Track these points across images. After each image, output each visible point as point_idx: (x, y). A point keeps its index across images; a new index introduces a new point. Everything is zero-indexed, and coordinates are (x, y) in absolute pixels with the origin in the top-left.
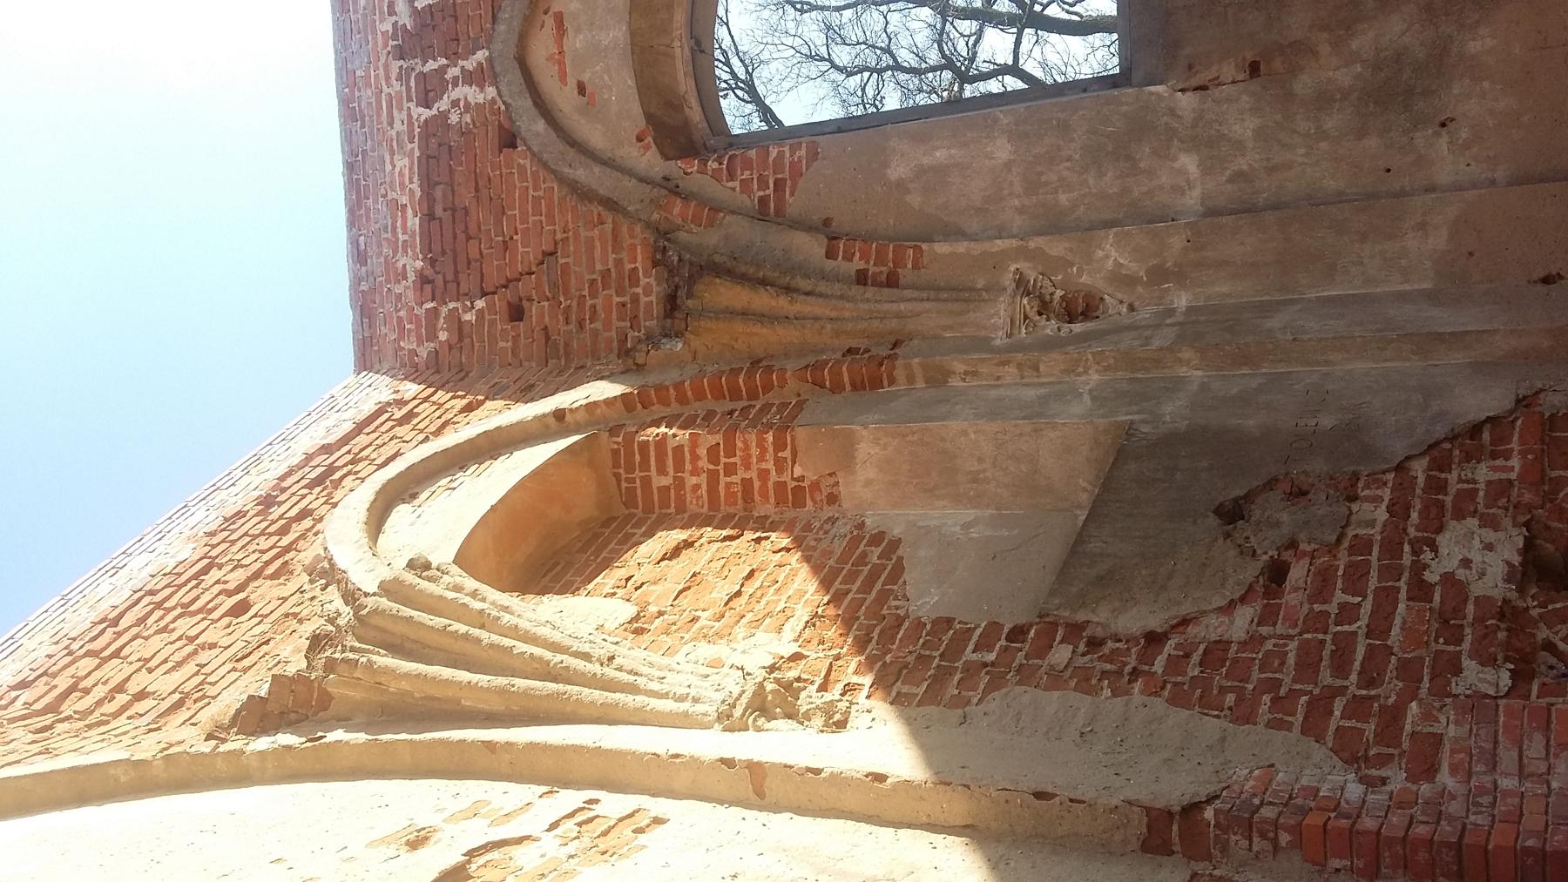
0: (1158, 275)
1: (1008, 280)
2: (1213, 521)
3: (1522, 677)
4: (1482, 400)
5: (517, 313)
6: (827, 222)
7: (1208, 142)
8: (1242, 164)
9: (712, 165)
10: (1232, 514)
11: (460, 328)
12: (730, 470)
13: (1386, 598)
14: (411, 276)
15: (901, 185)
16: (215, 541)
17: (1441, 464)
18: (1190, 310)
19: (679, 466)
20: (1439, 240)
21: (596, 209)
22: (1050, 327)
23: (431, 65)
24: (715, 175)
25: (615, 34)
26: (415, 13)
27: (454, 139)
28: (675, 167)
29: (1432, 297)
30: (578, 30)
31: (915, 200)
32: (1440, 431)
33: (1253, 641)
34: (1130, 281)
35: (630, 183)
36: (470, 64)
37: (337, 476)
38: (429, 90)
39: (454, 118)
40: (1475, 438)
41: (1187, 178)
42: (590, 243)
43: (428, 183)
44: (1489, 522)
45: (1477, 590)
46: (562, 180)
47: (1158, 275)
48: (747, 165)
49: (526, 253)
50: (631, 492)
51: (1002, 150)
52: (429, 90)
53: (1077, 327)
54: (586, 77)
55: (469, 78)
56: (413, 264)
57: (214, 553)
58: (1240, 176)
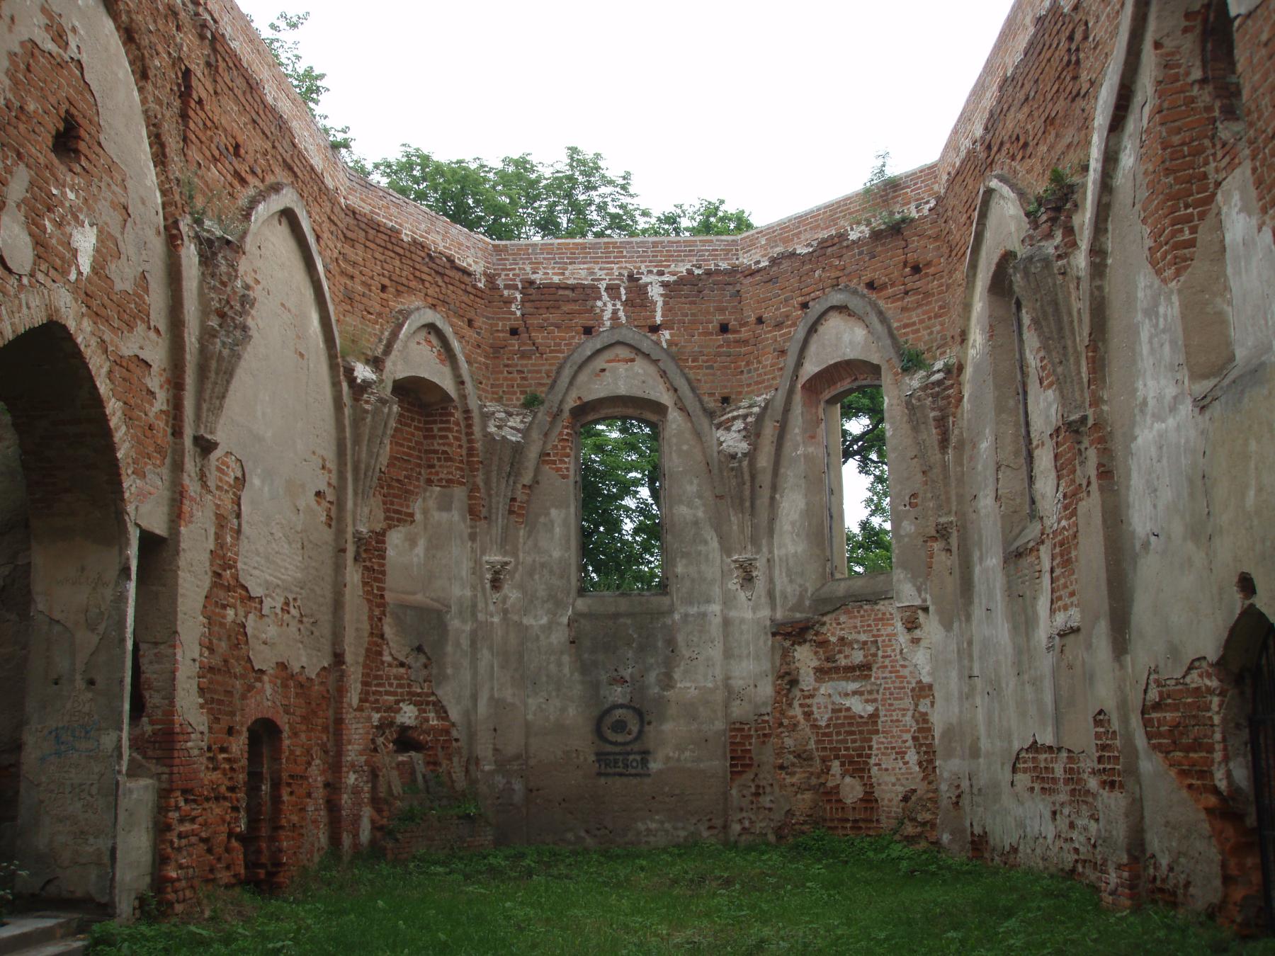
0: (505, 612)
1: (506, 559)
2: (417, 644)
3: (377, 727)
4: (454, 714)
5: (514, 332)
6: (537, 483)
7: (548, 628)
8: (542, 637)
9: (566, 431)
10: (419, 649)
11: (508, 302)
12: (439, 459)
13: (394, 694)
14: (533, 277)
15: (548, 514)
16: (413, 249)
17: (434, 704)
18: (492, 623)
19: (442, 437)
20: (510, 700)
21: (553, 375)
22: (489, 576)
23: (623, 291)
24: (561, 433)
25: (622, 390)
26: (646, 285)
27: (590, 303)
28: (566, 414)
29: (491, 698)
30: (626, 370)
31: (542, 519)
32: (445, 703)
33: (383, 663)
34: (504, 602)
35: (560, 397)
36: (621, 314)
37: (440, 283)
38: (612, 290)
39: (599, 303)
40: (442, 712)
41: (537, 620)
42: (539, 372)
43: (573, 288)
44: (417, 718)
45: (398, 716)
46: (569, 357)
47: (505, 612)
48: (564, 448)
49: (539, 337)
50: (432, 415)
51: (556, 554)
52: (612, 290)
53: (488, 586)
54: (607, 373)
55: (615, 312)
56: (538, 277)
57: (408, 254)
58: (538, 637)
